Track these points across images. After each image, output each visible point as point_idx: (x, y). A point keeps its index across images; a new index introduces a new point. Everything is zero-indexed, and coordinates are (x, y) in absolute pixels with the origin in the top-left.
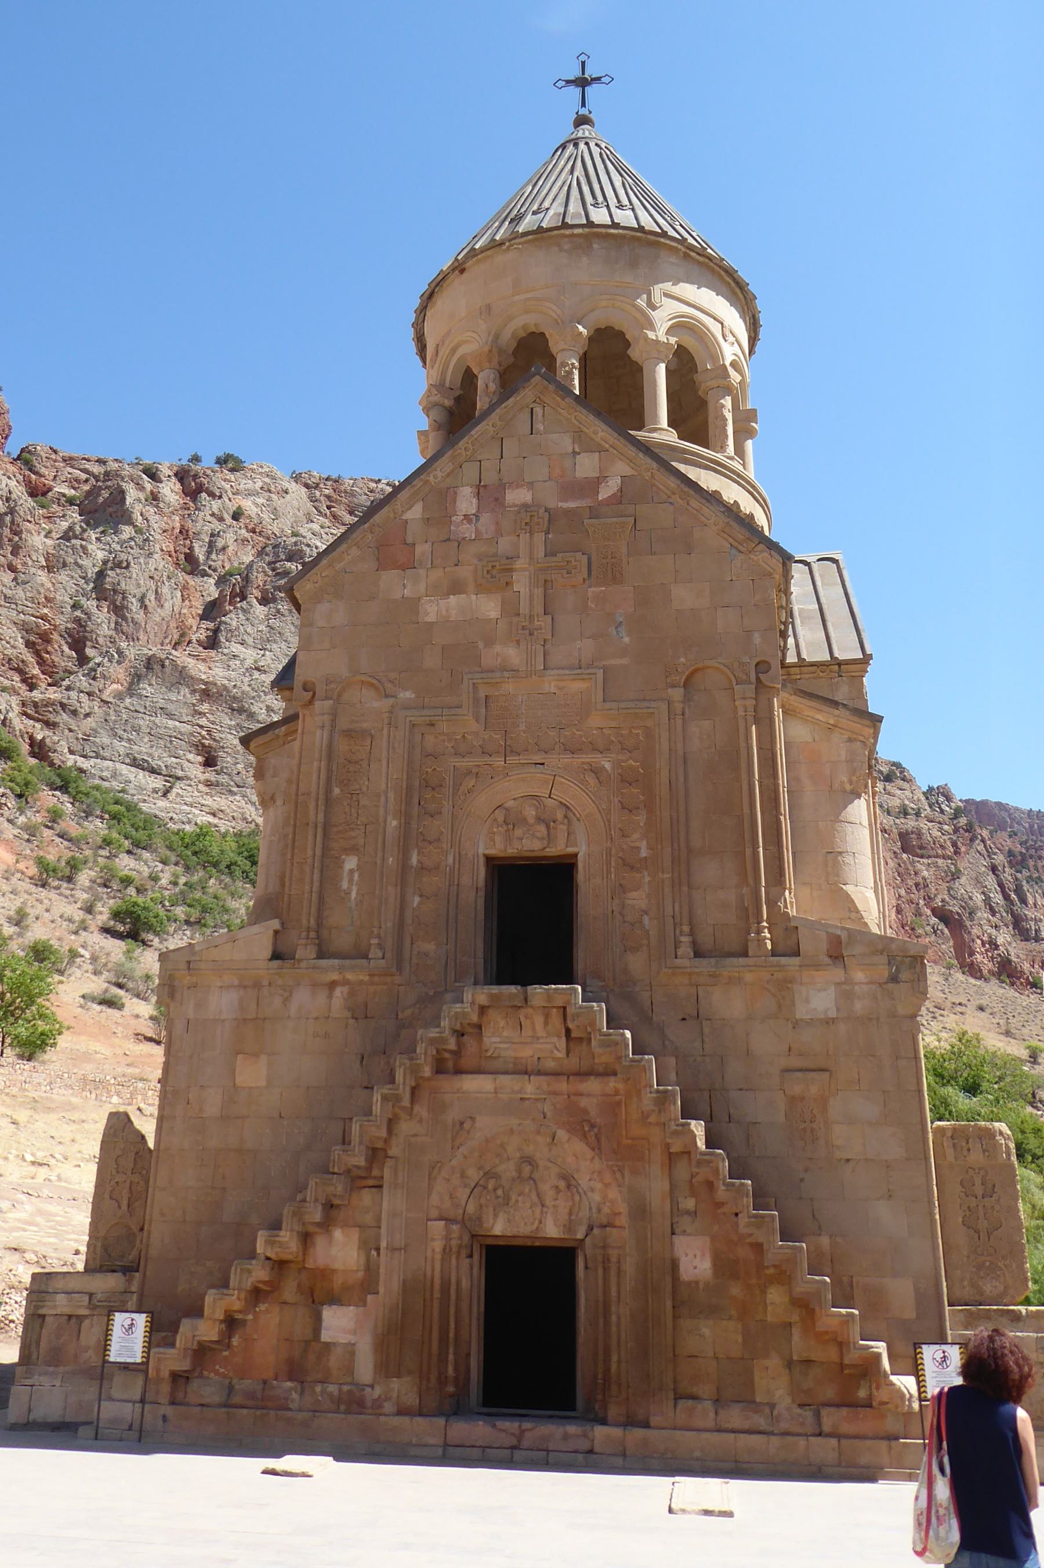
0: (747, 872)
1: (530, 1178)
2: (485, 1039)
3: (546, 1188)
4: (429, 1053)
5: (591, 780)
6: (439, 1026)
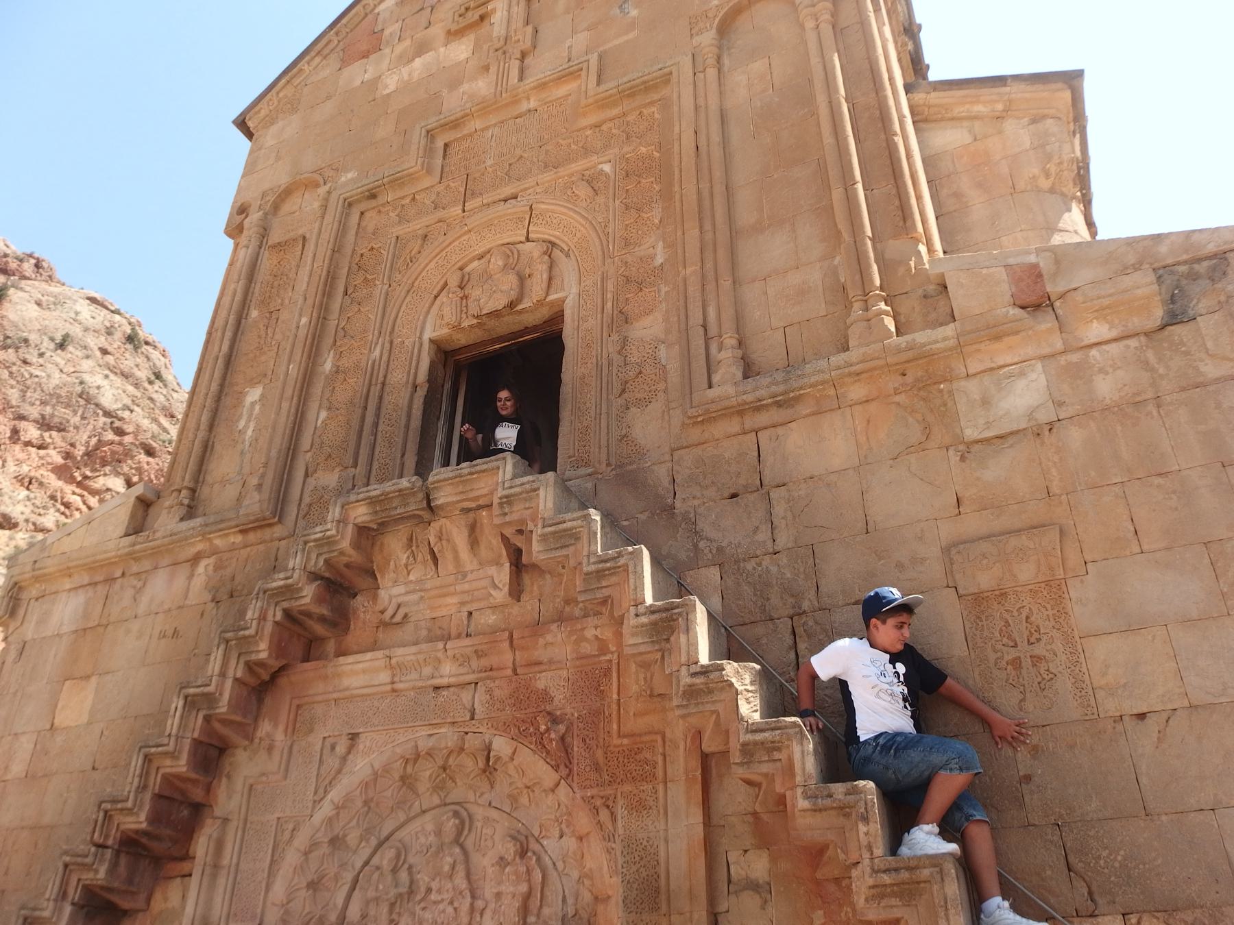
0: (839, 231)
2: (383, 594)
3: (485, 863)
4: (270, 617)
5: (583, 191)
6: (286, 569)
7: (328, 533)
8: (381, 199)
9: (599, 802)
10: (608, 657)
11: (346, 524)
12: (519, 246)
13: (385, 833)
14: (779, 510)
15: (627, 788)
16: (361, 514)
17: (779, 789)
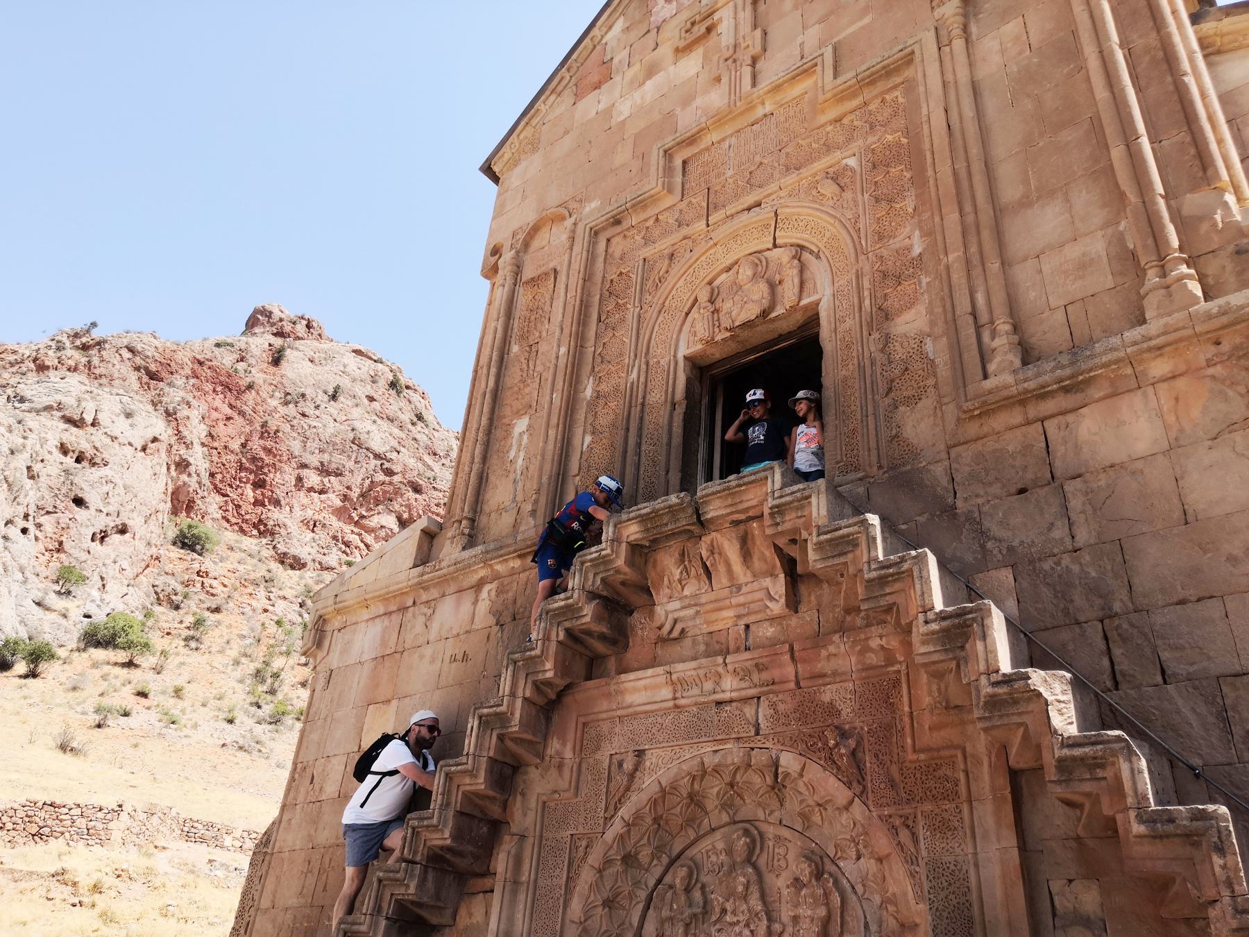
3: (780, 883)
5: (829, 189)
6: (565, 590)
7: (603, 553)
8: (625, 225)
9: (897, 822)
10: (895, 668)
11: (620, 543)
12: (767, 254)
13: (677, 849)
14: (1076, 503)
15: (928, 807)
16: (633, 531)
17: (1107, 811)
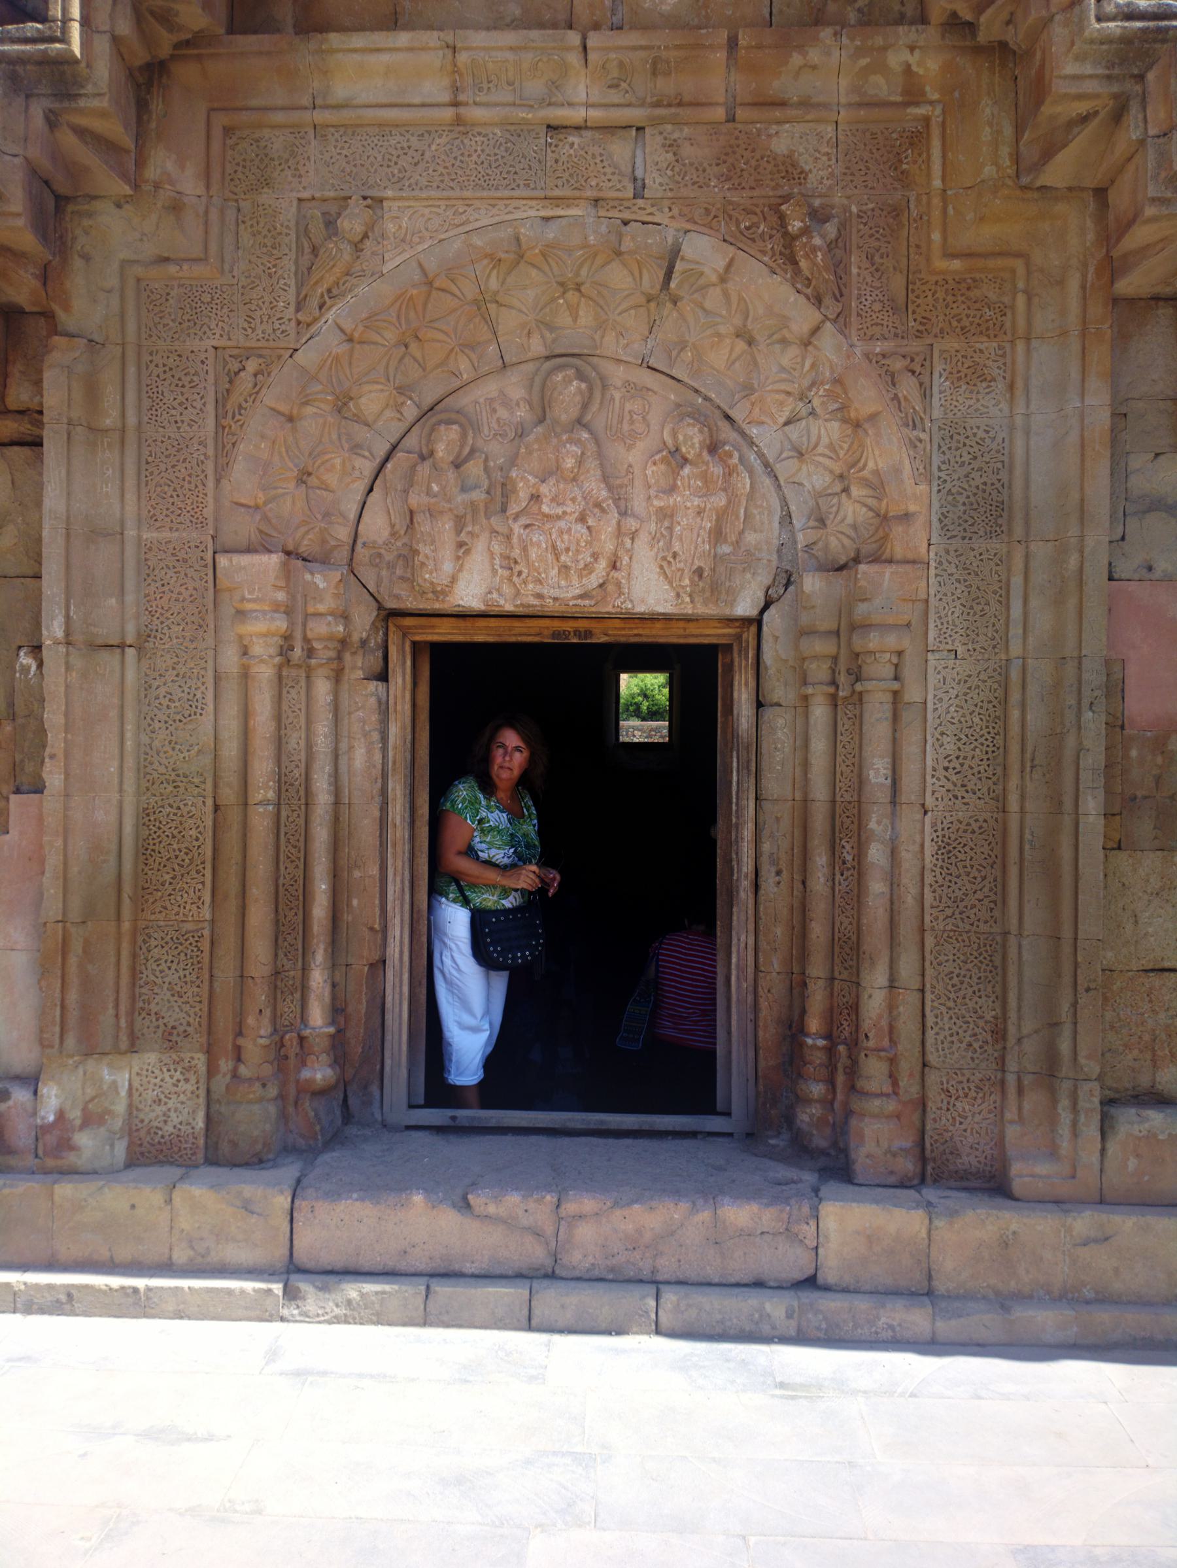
1: (579, 422)
9: (898, 365)
13: (428, 401)
